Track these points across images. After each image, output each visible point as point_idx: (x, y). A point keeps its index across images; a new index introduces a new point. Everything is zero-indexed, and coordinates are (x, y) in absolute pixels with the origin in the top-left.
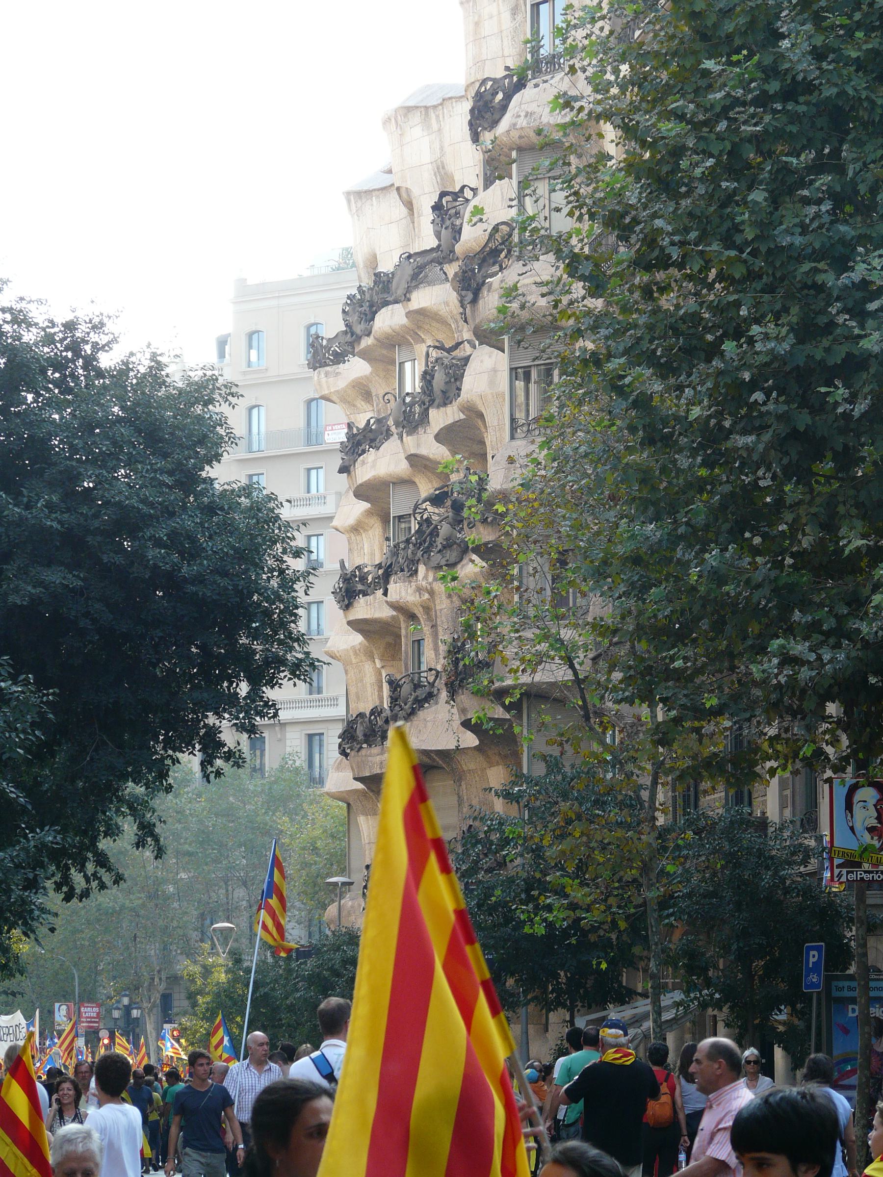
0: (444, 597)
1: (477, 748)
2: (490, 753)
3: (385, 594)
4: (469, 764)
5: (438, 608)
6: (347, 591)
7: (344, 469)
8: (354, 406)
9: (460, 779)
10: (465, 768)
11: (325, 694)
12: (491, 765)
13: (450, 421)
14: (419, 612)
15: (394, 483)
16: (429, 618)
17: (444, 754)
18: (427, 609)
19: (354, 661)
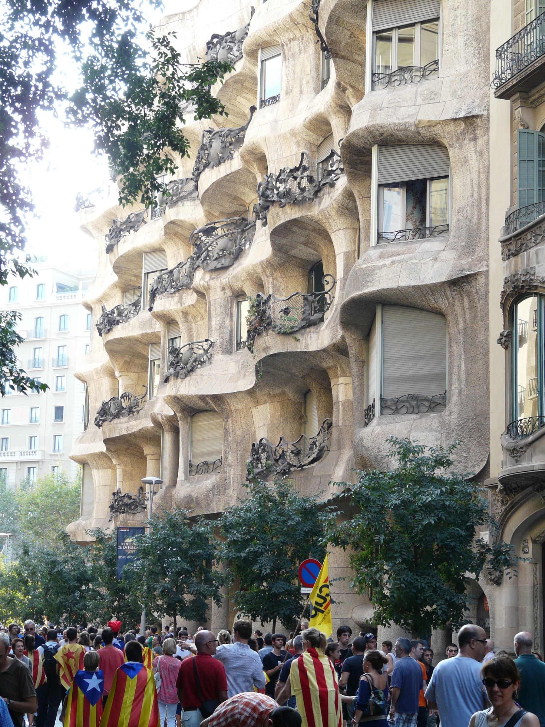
0: (218, 290)
1: (250, 392)
2: (259, 394)
3: (151, 309)
4: (235, 405)
5: (211, 299)
6: (109, 322)
7: (110, 249)
8: (102, 231)
9: (227, 417)
10: (233, 408)
11: (9, 451)
13: (223, 175)
14: (179, 318)
15: (146, 253)
16: (187, 321)
17: (218, 399)
18: (185, 314)
19: (95, 377)
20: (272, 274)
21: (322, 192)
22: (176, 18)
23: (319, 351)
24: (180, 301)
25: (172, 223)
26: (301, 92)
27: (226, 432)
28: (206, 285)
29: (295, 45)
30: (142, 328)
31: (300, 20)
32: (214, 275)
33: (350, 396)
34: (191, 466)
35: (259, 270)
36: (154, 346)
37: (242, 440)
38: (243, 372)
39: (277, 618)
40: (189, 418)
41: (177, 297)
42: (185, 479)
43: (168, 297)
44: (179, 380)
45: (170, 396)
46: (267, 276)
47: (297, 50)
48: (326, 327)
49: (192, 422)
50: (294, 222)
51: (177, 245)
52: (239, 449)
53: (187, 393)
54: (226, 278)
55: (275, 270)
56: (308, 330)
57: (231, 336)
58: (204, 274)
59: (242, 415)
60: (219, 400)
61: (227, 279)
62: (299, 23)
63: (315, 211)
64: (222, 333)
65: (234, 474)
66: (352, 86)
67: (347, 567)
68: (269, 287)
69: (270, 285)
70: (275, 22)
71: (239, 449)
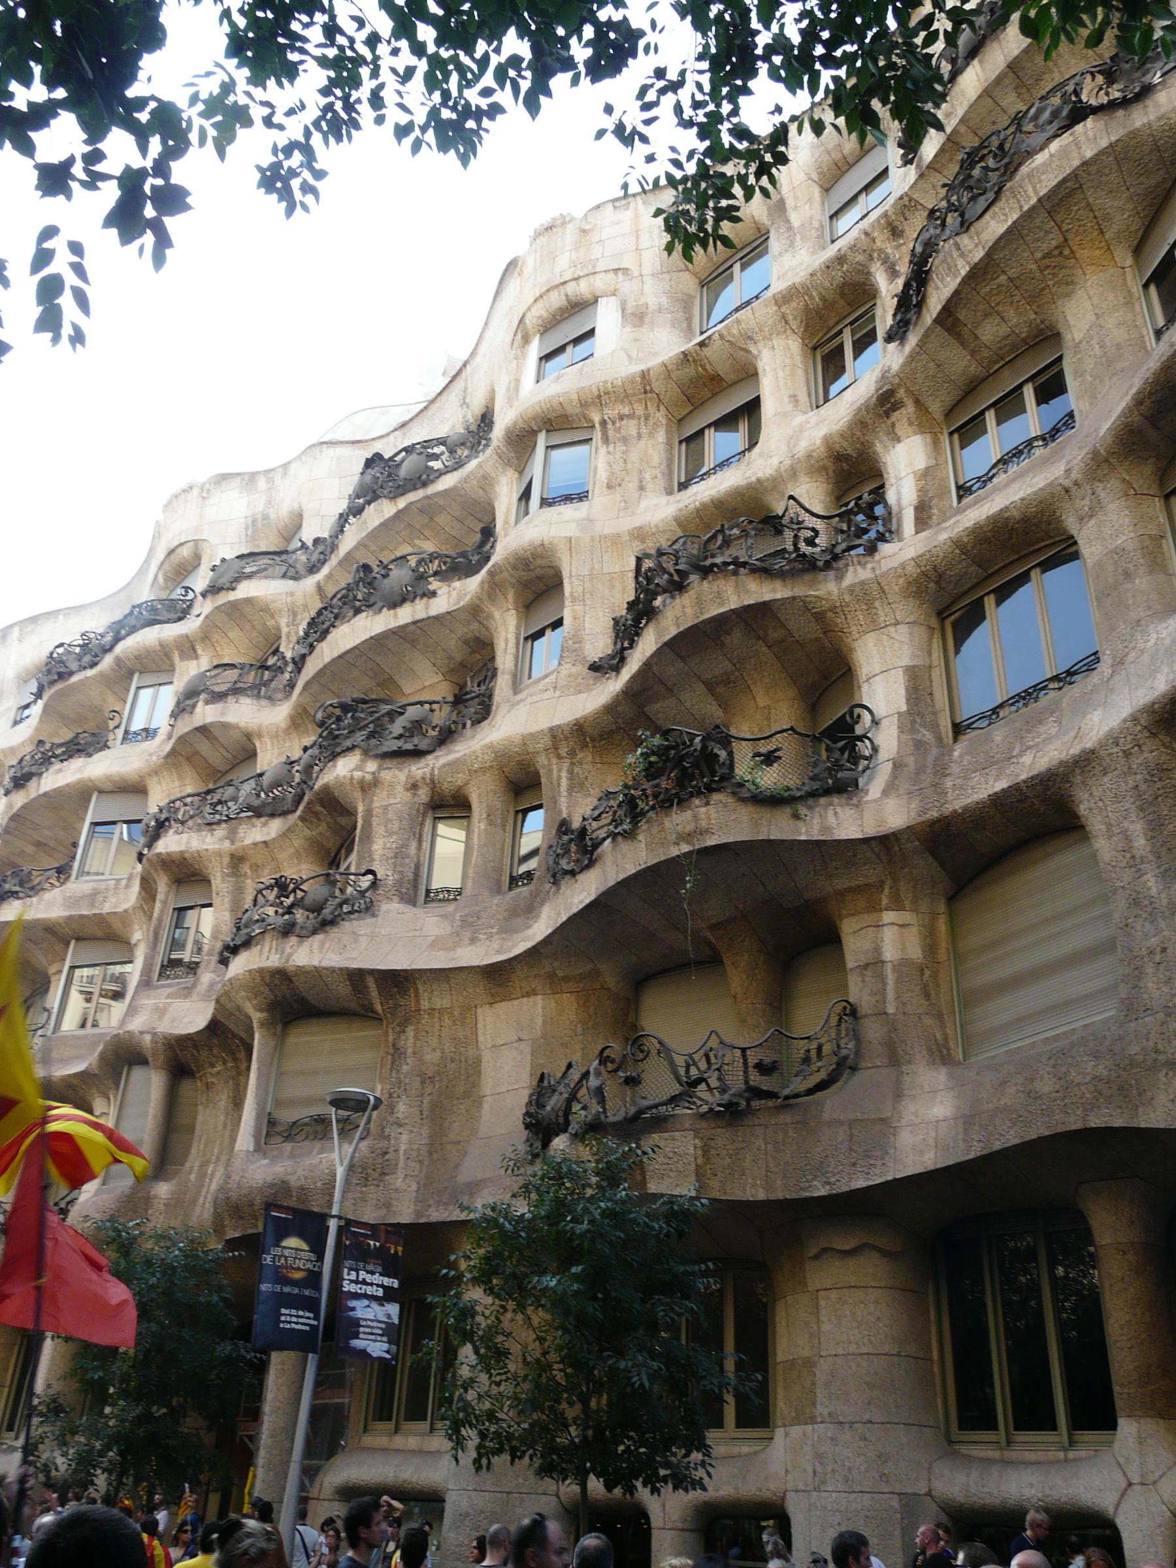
0: (400, 789)
4: (432, 998)
5: (376, 804)
12: (495, 999)
15: (101, 792)
17: (397, 982)
20: (572, 753)
21: (841, 563)
22: (236, 482)
23: (866, 841)
24: (232, 836)
25: (203, 730)
26: (642, 488)
27: (397, 1053)
28: (368, 777)
29: (630, 427)
30: (69, 907)
31: (657, 386)
32: (388, 763)
33: (915, 952)
34: (272, 1123)
35: (546, 741)
36: (82, 944)
37: (438, 1073)
38: (468, 934)
39: (639, 1484)
40: (280, 1027)
41: (221, 831)
42: (258, 1149)
43: (199, 830)
44: (293, 940)
45: (261, 971)
46: (559, 757)
47: (634, 432)
48: (886, 793)
49: (284, 1036)
50: (763, 609)
51: (181, 777)
52: (428, 1090)
53: (316, 963)
54: (419, 769)
55: (584, 746)
56: (823, 800)
57: (417, 875)
58: (362, 761)
59: (447, 1021)
60: (398, 984)
61: (427, 770)
62: (652, 391)
63: (828, 589)
64: (402, 865)
65: (410, 1143)
66: (918, 403)
67: (899, 1355)
68: (559, 778)
69: (564, 774)
70: (605, 382)
71: (428, 1090)
